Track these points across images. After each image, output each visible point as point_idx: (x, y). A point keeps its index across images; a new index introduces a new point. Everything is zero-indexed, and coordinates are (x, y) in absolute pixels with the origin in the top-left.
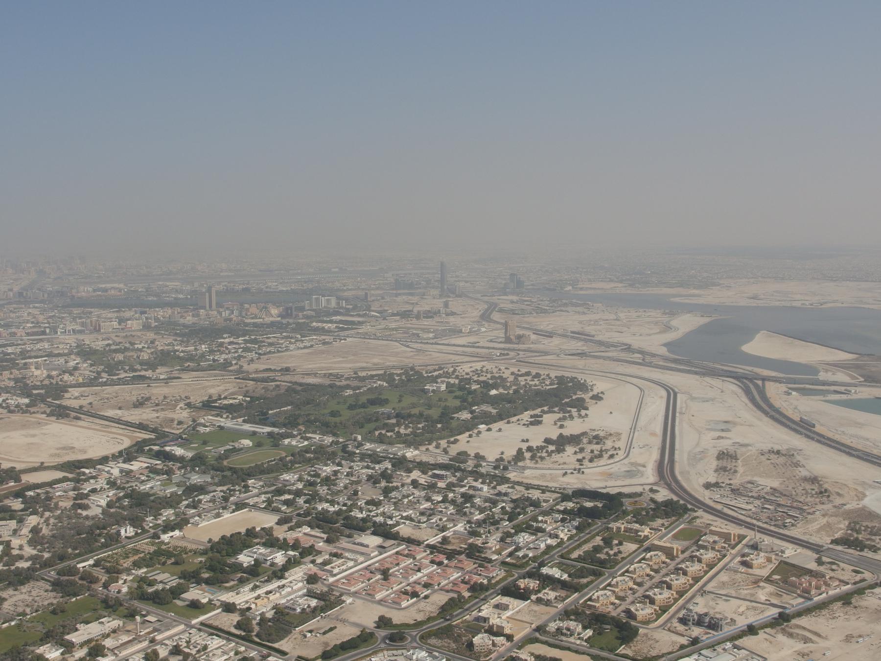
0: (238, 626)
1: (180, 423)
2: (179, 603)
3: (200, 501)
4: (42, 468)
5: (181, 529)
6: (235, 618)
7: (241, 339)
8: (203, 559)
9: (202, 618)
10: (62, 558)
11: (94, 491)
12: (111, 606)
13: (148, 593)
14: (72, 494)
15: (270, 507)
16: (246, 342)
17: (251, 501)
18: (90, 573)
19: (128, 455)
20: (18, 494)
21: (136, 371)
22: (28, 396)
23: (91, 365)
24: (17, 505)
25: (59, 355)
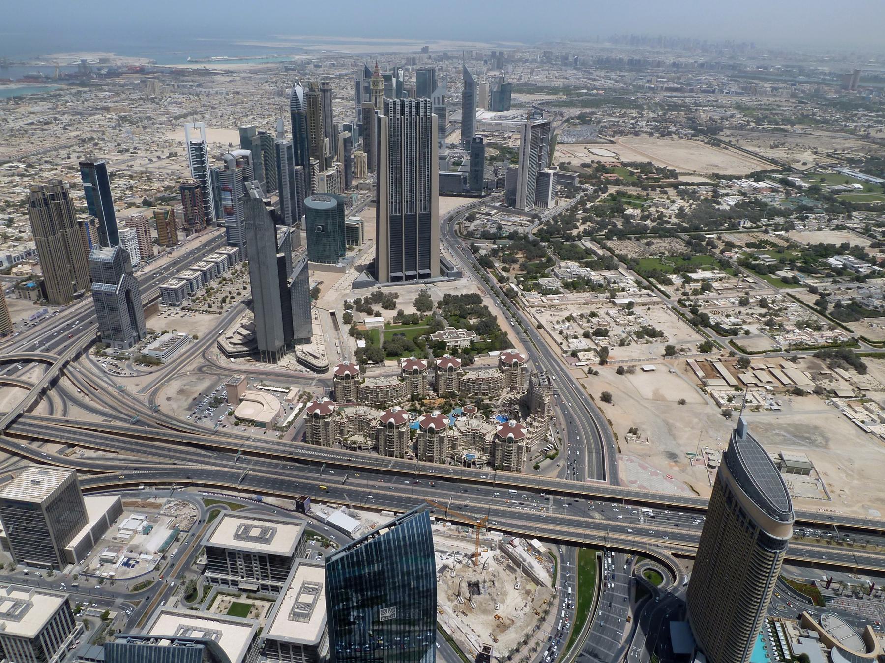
0: (816, 303)
1: (804, 164)
2: (773, 276)
3: (807, 217)
4: (694, 174)
5: (787, 231)
6: (816, 297)
7: (873, 114)
8: (800, 254)
9: (788, 290)
10: (697, 229)
11: (727, 195)
12: (724, 265)
13: (750, 263)
14: (711, 194)
15: (866, 232)
16: (878, 116)
17: (850, 226)
18: (713, 242)
19: (758, 176)
20: (675, 186)
21: (777, 124)
22: (694, 129)
23: (744, 116)
24: (671, 192)
25: (722, 107)
